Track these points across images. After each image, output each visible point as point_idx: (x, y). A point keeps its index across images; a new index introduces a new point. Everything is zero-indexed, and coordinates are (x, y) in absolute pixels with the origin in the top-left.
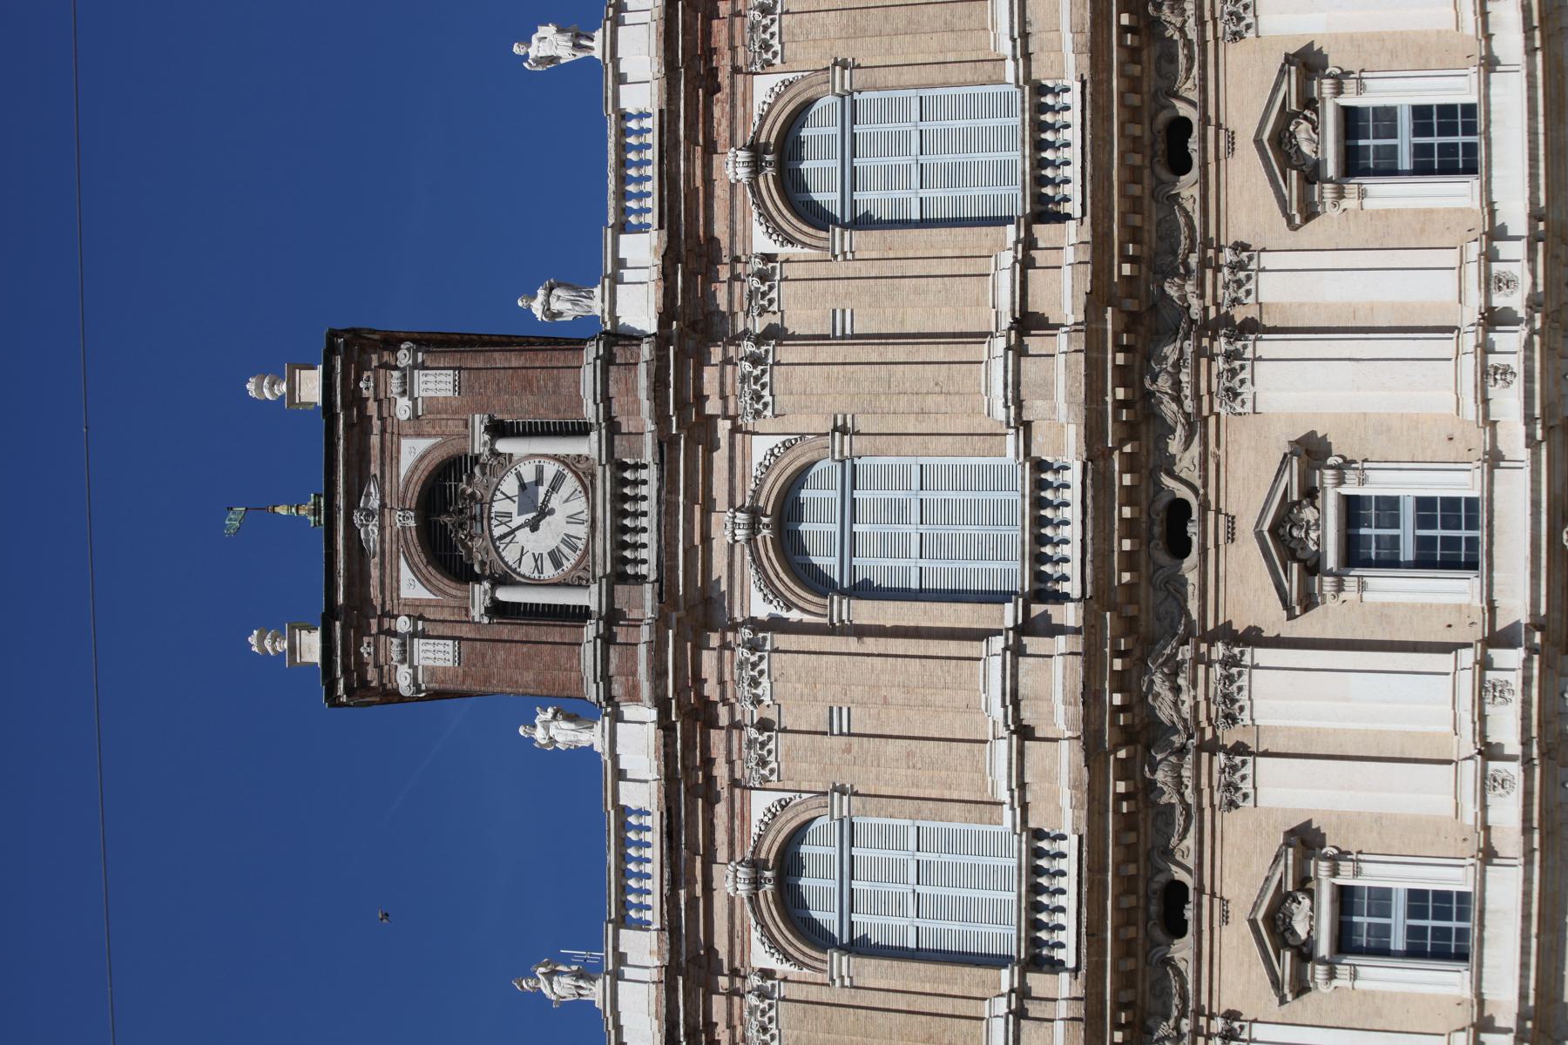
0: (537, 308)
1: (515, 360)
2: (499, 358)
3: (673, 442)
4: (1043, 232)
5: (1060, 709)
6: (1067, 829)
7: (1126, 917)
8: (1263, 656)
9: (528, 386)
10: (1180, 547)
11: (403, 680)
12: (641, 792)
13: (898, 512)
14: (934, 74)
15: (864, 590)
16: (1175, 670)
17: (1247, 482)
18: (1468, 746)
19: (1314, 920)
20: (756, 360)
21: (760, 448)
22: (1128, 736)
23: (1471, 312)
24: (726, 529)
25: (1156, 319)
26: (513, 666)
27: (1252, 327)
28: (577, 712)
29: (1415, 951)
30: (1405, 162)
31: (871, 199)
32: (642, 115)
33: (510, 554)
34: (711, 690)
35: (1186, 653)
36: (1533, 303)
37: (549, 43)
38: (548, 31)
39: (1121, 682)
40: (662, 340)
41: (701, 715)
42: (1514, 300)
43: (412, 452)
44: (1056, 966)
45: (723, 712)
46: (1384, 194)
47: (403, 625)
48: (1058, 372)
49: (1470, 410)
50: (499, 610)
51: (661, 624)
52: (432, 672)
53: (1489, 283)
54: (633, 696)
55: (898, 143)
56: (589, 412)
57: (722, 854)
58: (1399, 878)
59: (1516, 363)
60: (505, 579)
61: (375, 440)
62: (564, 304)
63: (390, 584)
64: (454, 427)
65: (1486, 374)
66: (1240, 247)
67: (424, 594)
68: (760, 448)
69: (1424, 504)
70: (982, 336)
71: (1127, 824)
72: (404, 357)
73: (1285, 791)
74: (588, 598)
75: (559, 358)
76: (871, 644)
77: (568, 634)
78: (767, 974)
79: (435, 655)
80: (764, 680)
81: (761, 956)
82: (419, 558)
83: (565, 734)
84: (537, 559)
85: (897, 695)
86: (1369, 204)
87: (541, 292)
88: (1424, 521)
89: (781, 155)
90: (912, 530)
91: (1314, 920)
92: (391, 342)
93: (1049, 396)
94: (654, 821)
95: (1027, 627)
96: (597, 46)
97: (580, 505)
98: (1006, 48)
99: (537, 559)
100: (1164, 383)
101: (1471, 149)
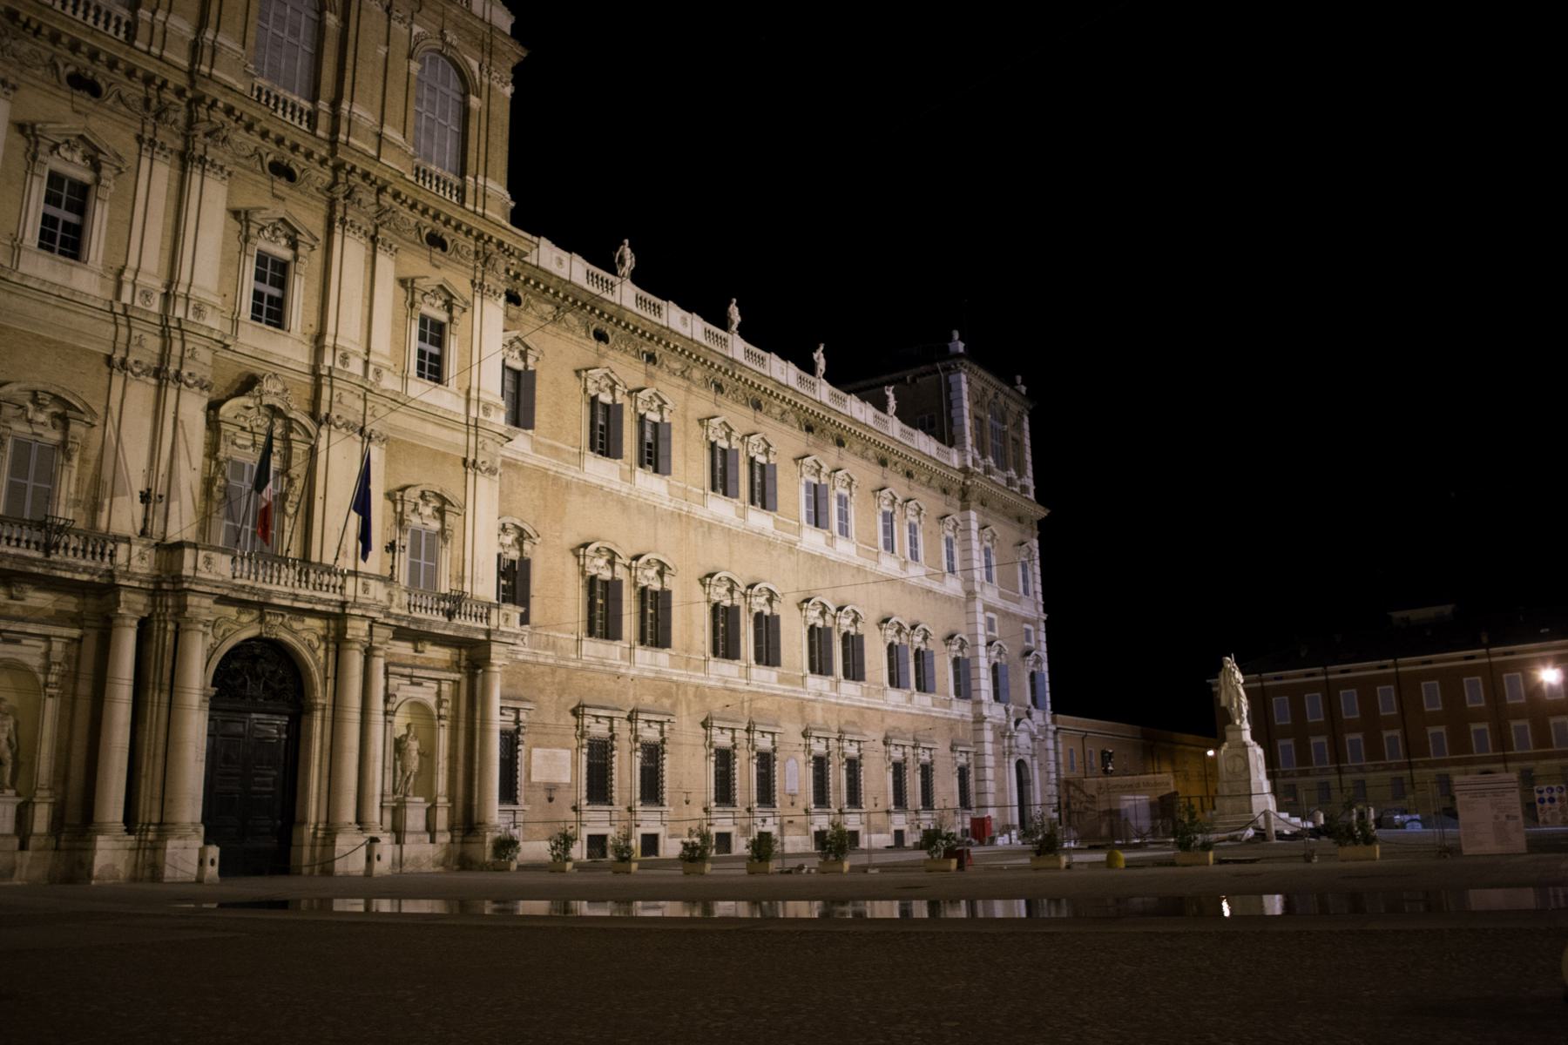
55: (444, 115)
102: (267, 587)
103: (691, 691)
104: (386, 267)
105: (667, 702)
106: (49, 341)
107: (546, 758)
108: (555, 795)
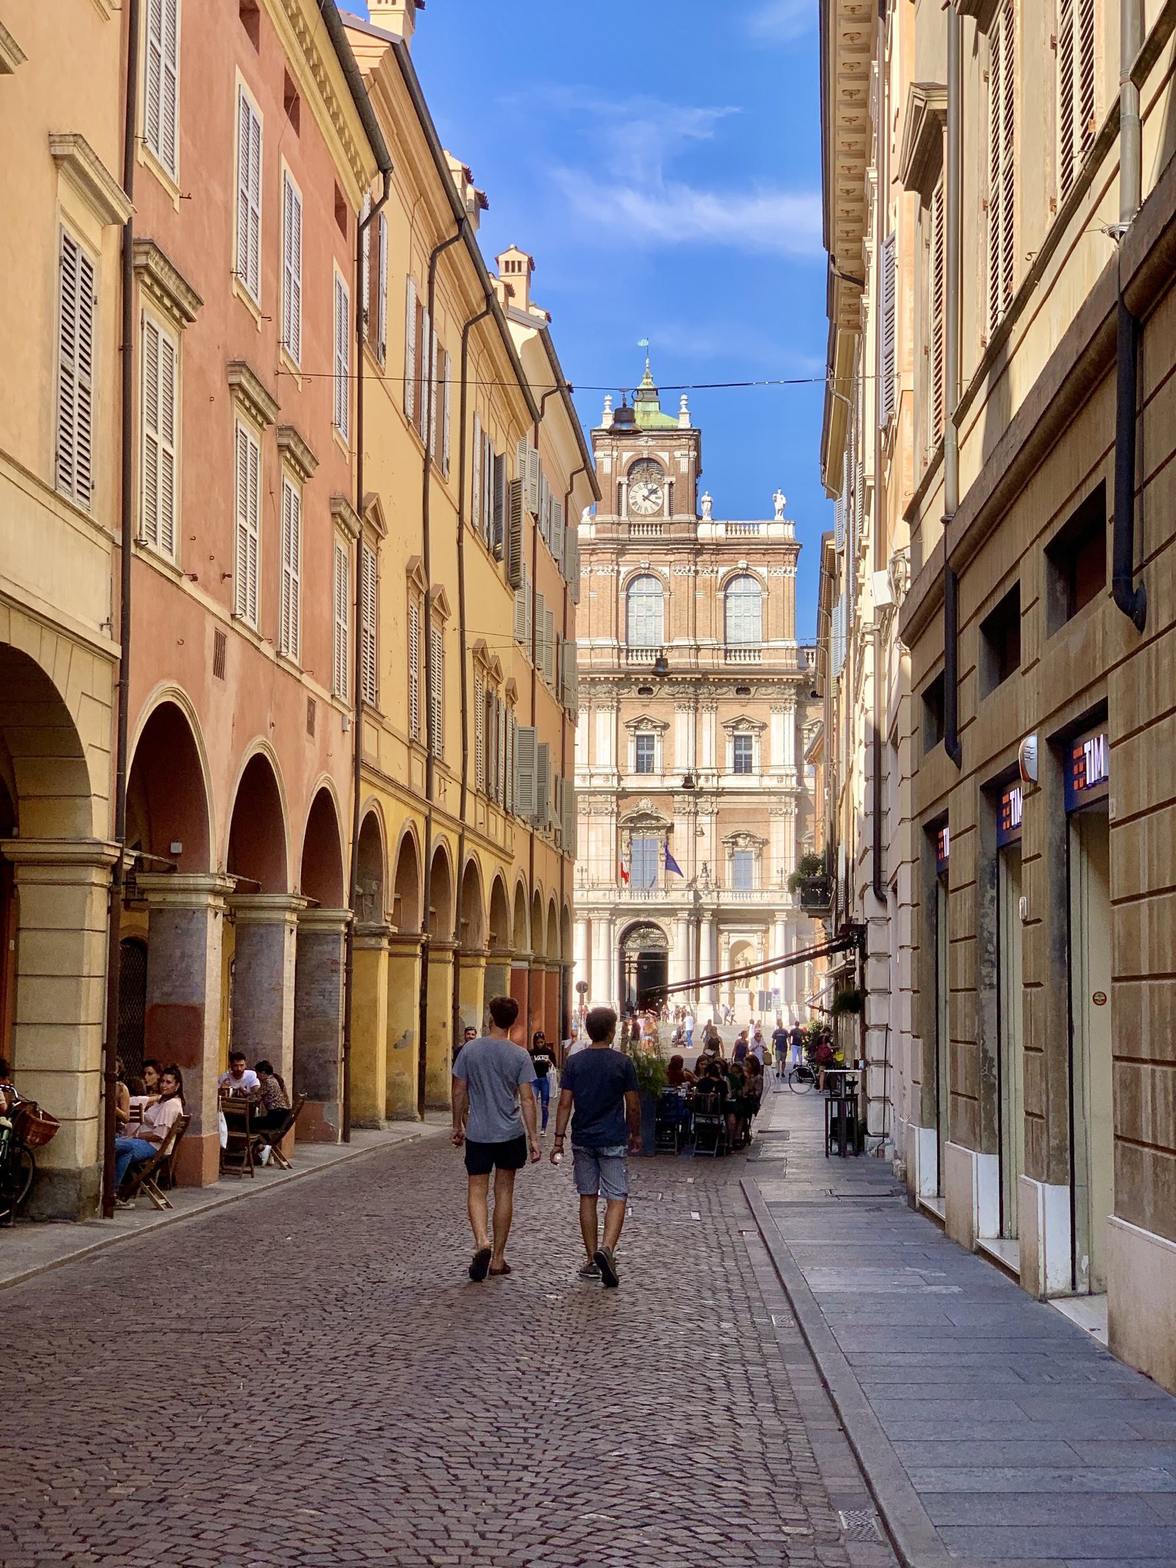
0: (705, 498)
4: (722, 653)
8: (614, 716)
9: (683, 497)
10: (641, 691)
15: (628, 597)
17: (656, 711)
24: (644, 561)
25: (700, 686)
27: (696, 709)
31: (731, 602)
33: (635, 488)
34: (601, 556)
37: (780, 501)
38: (784, 501)
43: (664, 456)
45: (594, 558)
47: (615, 454)
49: (676, 771)
50: (620, 485)
52: (602, 463)
53: (707, 776)
54: (598, 531)
56: (676, 517)
60: (628, 485)
61: (668, 442)
62: (706, 507)
63: (628, 448)
67: (624, 460)
68: (666, 570)
72: (693, 454)
76: (614, 605)
77: (614, 509)
84: (634, 497)
85: (601, 613)
87: (709, 499)
92: (697, 448)
95: (620, 650)
96: (779, 517)
97: (650, 512)
99: (634, 497)
104: (708, 719)
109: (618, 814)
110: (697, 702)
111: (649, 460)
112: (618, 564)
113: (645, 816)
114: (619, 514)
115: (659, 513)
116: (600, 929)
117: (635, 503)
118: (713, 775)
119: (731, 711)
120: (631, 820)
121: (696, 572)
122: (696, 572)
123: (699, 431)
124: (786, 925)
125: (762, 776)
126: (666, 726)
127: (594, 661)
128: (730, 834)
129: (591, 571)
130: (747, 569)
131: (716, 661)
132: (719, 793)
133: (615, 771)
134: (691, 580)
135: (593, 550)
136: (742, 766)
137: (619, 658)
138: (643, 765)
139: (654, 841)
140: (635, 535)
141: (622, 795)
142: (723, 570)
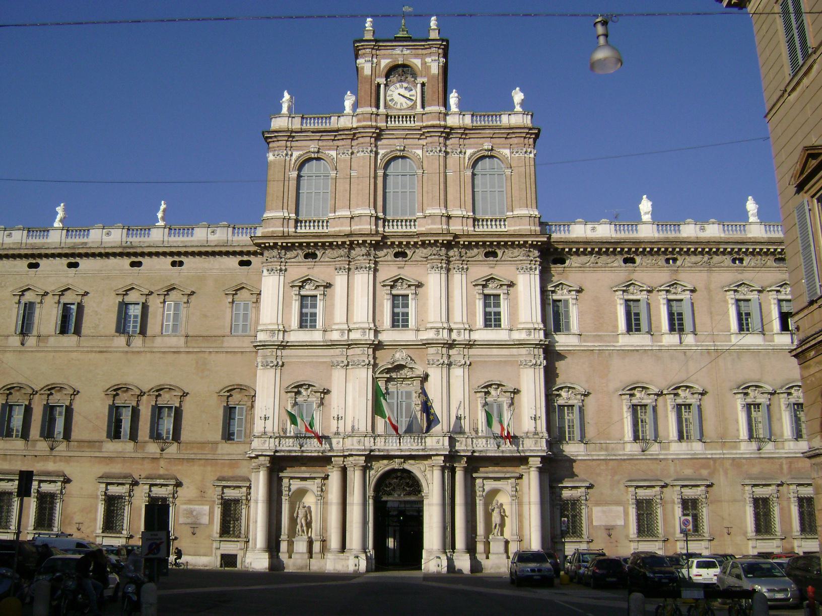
1: (441, 89)
2: (441, 85)
3: (420, 130)
4: (470, 221)
5: (358, 227)
6: (329, 229)
7: (308, 244)
8: (371, 276)
10: (397, 255)
11: (360, 61)
12: (336, 122)
13: (404, 186)
14: (509, 195)
16: (369, 254)
17: (410, 272)
18: (351, 326)
19: (308, 290)
20: (440, 151)
21: (419, 152)
22: (352, 242)
23: (453, 326)
25: (450, 248)
26: (365, 89)
28: (355, 106)
29: (302, 315)
30: (488, 310)
32: (500, 121)
33: (392, 88)
35: (372, 258)
36: (454, 340)
37: (518, 96)
39: (364, 242)
40: (445, 127)
41: (354, 137)
42: (454, 335)
43: (417, 62)
44: (296, 227)
45: (354, 143)
46: (480, 305)
47: (375, 60)
48: (437, 226)
50: (379, 85)
51: (377, 128)
52: (363, 68)
54: (359, 121)
57: (320, 143)
58: (319, 310)
59: (440, 336)
61: (420, 52)
63: (385, 57)
64: (424, 73)
65: (437, 329)
66: (467, 269)
68: (419, 152)
69: (407, 314)
70: (446, 207)
71: (331, 243)
72: (442, 60)
73: (340, 281)
74: (382, 110)
75: (441, 101)
76: (372, 180)
77: (373, 104)
78: (291, 155)
79: (367, 69)
80: (362, 154)
81: (296, 154)
82: (391, 65)
83: (348, 103)
86: (477, 301)
88: (403, 314)
89: (490, 156)
90: (400, 190)
91: (308, 290)
92: (445, 56)
93: (433, 223)
94: (328, 127)
95: (377, 218)
97: (405, 106)
98: (515, 213)
100: (435, 252)
101: (490, 326)
102: (387, 448)
103: (727, 464)
105: (705, 472)
106: (306, 362)
107: (604, 512)
108: (611, 532)
109: (375, 365)
110: (449, 262)
111: (404, 66)
112: (376, 146)
113: (400, 367)
114: (378, 107)
115: (413, 107)
116: (355, 479)
117: (392, 100)
118: (465, 329)
119: (480, 271)
120: (388, 371)
121: (447, 153)
122: (447, 153)
123: (447, 41)
124: (541, 471)
125: (511, 330)
126: (419, 285)
127: (353, 228)
128: (482, 381)
129: (352, 153)
130: (492, 150)
131: (465, 228)
132: (470, 345)
133: (372, 326)
134: (442, 159)
135: (354, 134)
136: (492, 320)
137: (377, 225)
138: (399, 321)
139: (409, 395)
140: (391, 124)
141: (378, 346)
142: (469, 152)
